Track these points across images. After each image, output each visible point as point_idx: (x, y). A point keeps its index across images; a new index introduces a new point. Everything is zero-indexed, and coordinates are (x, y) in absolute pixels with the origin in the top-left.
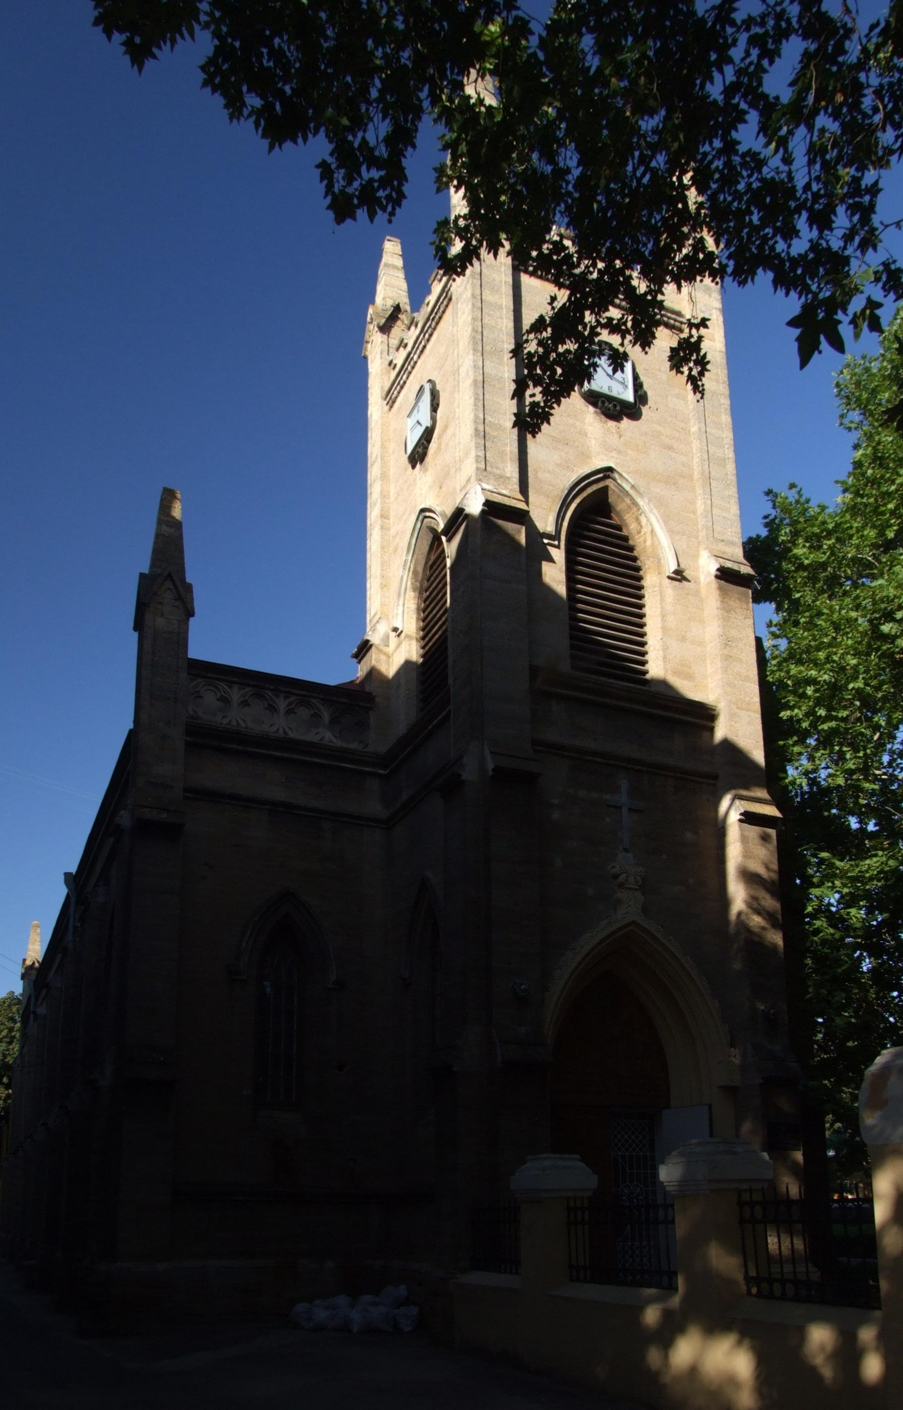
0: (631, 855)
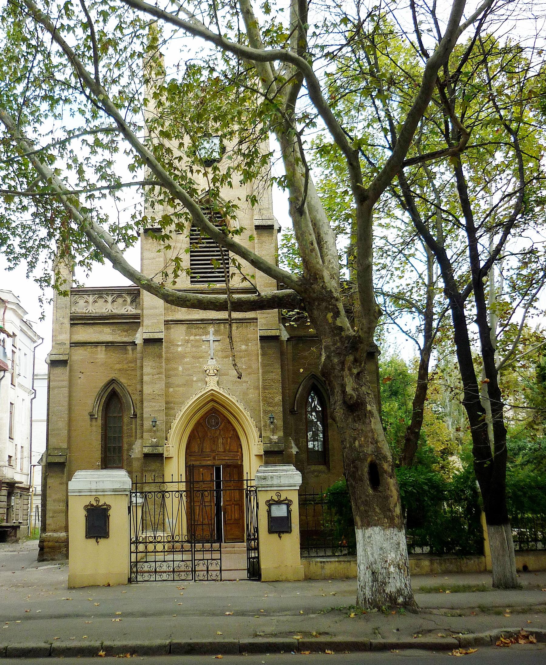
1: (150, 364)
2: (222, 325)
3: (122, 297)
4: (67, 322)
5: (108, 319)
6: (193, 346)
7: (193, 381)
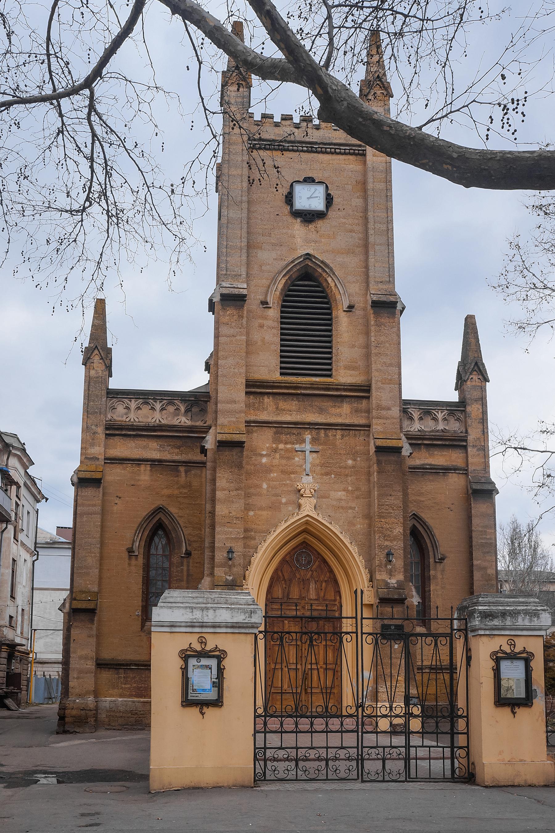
0: (311, 477)
1: (226, 476)
2: (323, 431)
3: (174, 404)
4: (100, 430)
5: (155, 431)
6: (282, 457)
7: (280, 503)
